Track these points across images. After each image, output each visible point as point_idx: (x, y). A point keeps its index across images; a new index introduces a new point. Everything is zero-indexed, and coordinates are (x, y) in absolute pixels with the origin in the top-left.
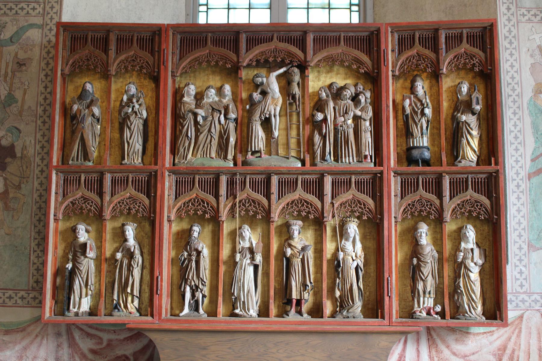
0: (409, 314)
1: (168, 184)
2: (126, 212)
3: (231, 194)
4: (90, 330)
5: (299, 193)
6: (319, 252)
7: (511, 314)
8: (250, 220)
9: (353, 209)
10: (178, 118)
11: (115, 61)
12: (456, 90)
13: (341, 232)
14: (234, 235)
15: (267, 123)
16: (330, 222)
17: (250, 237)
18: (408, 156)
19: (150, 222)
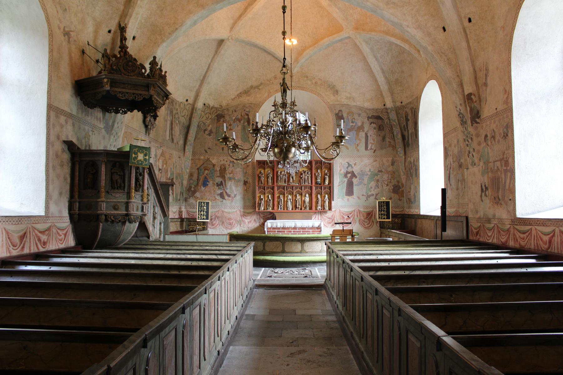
0: (316, 209)
1: (276, 188)
2: (269, 192)
3: (287, 190)
4: (263, 213)
5: (298, 189)
6: (301, 199)
7: (333, 210)
8: (290, 194)
9: (307, 192)
10: (277, 177)
11: (266, 166)
12: (325, 171)
13: (305, 196)
14: (287, 197)
15: (293, 178)
16: (303, 194)
17: (290, 197)
18: (316, 183)
19: (273, 195)
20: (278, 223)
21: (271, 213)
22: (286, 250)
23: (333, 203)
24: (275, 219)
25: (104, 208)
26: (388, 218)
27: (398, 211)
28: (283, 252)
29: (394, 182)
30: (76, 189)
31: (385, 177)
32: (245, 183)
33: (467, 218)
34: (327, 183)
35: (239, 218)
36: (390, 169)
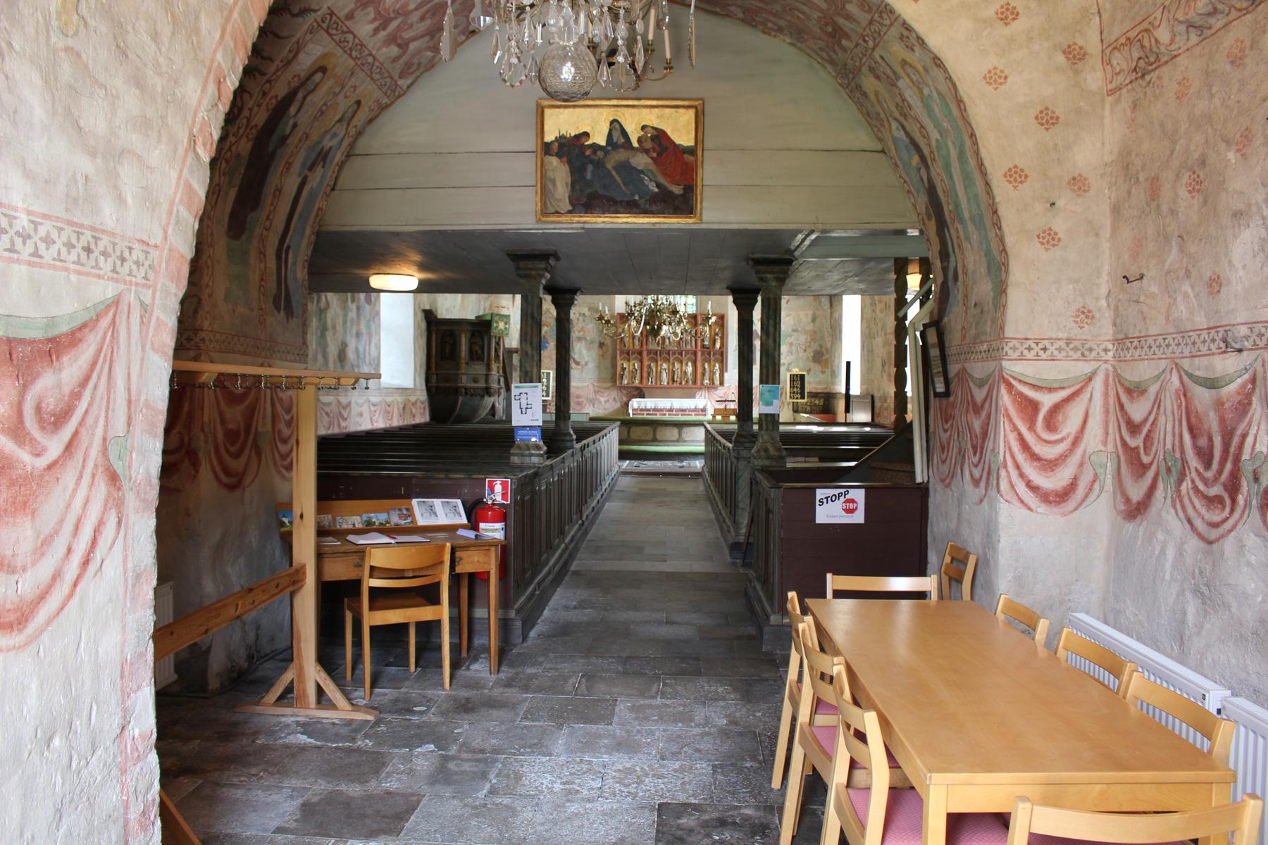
1: (645, 354)
4: (625, 388)
17: (665, 366)
18: (703, 346)
19: (641, 362)
20: (649, 403)
21: (638, 388)
22: (658, 437)
23: (726, 375)
24: (643, 397)
25: (465, 381)
26: (803, 397)
27: (820, 388)
28: (655, 441)
29: (815, 346)
30: (433, 360)
31: (803, 338)
32: (601, 345)
33: (873, 397)
34: (718, 345)
35: (592, 395)
36: (810, 327)
